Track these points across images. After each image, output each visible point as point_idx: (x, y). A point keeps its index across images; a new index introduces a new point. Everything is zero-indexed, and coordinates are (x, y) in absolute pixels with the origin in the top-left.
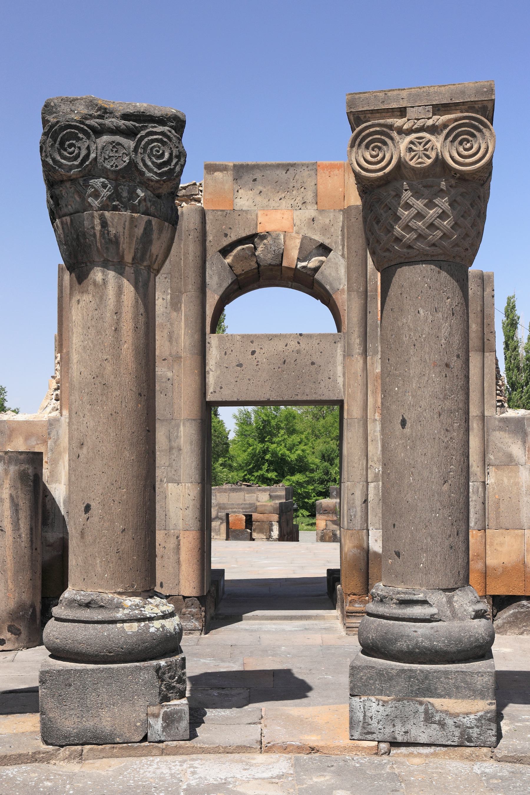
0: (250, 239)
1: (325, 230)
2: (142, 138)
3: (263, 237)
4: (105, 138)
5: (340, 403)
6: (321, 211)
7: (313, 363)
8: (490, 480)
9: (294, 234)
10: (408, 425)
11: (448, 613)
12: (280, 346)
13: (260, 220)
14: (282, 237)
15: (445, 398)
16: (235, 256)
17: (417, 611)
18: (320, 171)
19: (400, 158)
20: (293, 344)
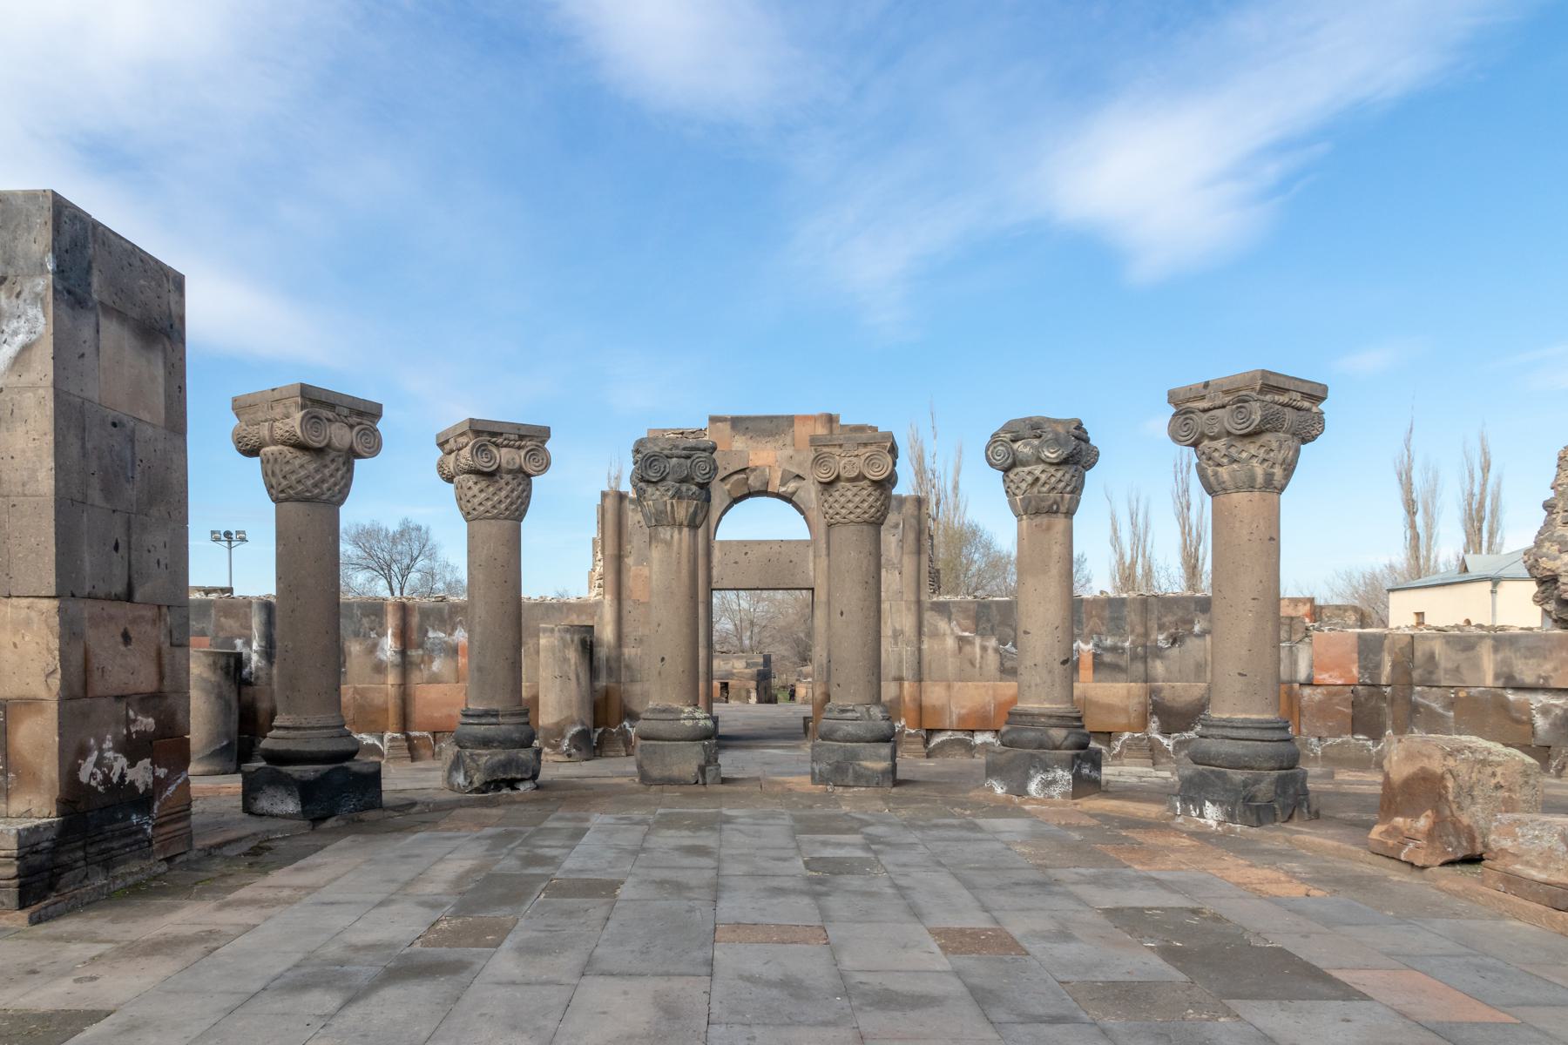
0: (743, 470)
1: (800, 465)
2: (693, 461)
3: (754, 470)
4: (674, 460)
5: (813, 589)
6: (797, 451)
7: (791, 561)
8: (925, 646)
9: (776, 468)
10: (844, 615)
11: (867, 716)
12: (767, 549)
13: (751, 457)
14: (767, 470)
15: (865, 600)
16: (732, 484)
17: (849, 715)
18: (796, 421)
19: (839, 473)
20: (776, 547)
